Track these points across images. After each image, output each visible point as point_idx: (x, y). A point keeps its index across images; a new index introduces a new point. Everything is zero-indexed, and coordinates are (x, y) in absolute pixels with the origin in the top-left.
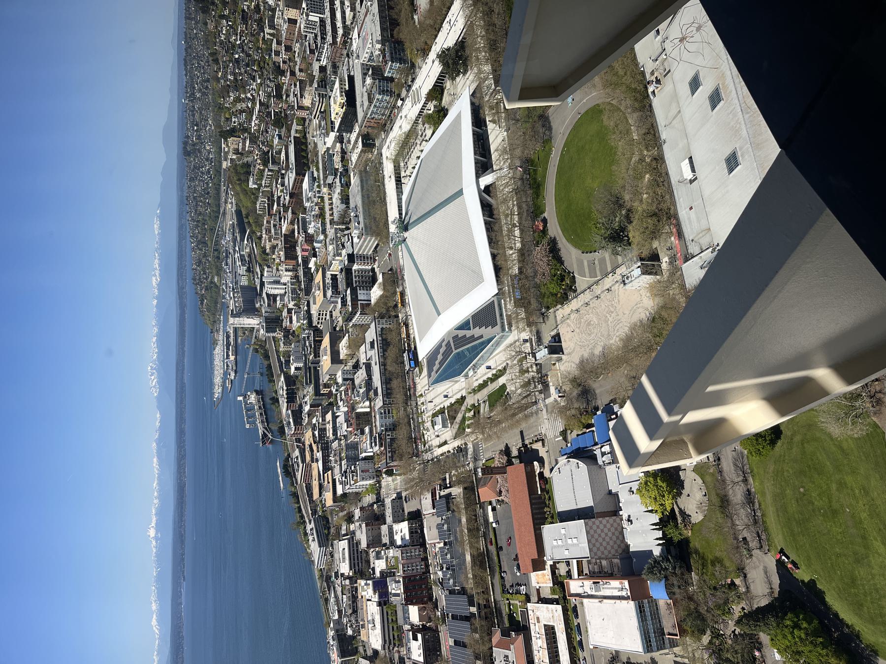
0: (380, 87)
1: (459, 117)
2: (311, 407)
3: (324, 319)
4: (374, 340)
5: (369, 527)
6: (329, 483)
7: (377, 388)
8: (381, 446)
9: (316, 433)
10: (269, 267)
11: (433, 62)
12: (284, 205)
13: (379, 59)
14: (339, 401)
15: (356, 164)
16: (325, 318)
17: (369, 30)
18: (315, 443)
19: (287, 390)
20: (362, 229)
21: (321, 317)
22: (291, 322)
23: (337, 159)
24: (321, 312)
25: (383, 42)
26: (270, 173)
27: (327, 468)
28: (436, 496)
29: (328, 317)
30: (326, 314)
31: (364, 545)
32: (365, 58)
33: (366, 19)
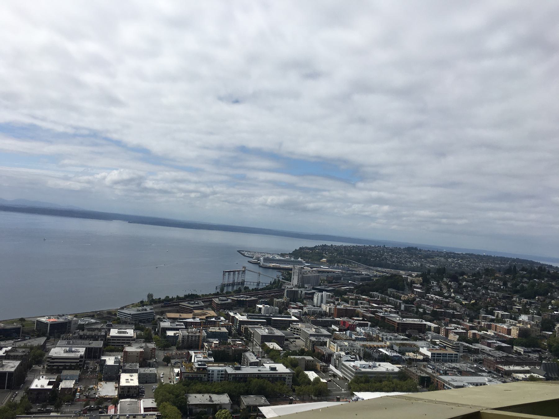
2: (232, 316)
3: (294, 332)
5: (139, 354)
6: (177, 325)
8: (198, 369)
9: (213, 319)
12: (377, 312)
15: (408, 370)
16: (295, 334)
18: (207, 318)
19: (246, 301)
20: (360, 370)
22: (294, 308)
23: (411, 355)
24: (299, 331)
26: (398, 304)
27: (187, 325)
28: (153, 411)
29: (296, 336)
30: (297, 334)
31: (128, 349)
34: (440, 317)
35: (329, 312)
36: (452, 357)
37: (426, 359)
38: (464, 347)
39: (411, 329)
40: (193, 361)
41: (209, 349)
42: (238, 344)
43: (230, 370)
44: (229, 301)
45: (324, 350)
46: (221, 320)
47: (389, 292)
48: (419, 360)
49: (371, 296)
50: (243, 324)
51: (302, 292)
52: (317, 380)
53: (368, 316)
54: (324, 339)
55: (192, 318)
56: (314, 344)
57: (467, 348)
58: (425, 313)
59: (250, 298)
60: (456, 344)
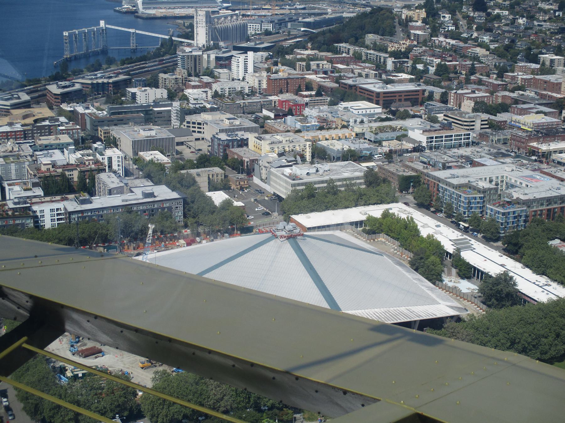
0: (475, 198)
1: (434, 302)
2: (81, 114)
3: (194, 129)
4: (155, 197)
7: (91, 203)
9: (47, 123)
10: (267, 59)
11: (502, 266)
12: (340, 77)
13: (507, 197)
14: (81, 152)
16: (195, 132)
17: (542, 183)
18: (36, 121)
19: (108, 83)
21: (196, 126)
22: (194, 87)
23: (394, 145)
24: (202, 126)
25: (528, 203)
26: (382, 60)
32: (510, 179)
33: (554, 181)
34: (452, 75)
35: (259, 87)
36: (461, 139)
37: (418, 149)
38: (482, 121)
39: (400, 100)
40: (8, 198)
41: (35, 175)
42: (87, 160)
43: (71, 205)
44: (77, 87)
45: (245, 154)
46: (60, 123)
47: (368, 42)
48: (407, 151)
49: (336, 51)
50: (102, 126)
51: (209, 56)
52: (227, 204)
53: (328, 88)
54: (243, 135)
55: (6, 125)
56: (227, 145)
57: (486, 122)
58: (426, 71)
59: (116, 77)
60: (469, 118)
